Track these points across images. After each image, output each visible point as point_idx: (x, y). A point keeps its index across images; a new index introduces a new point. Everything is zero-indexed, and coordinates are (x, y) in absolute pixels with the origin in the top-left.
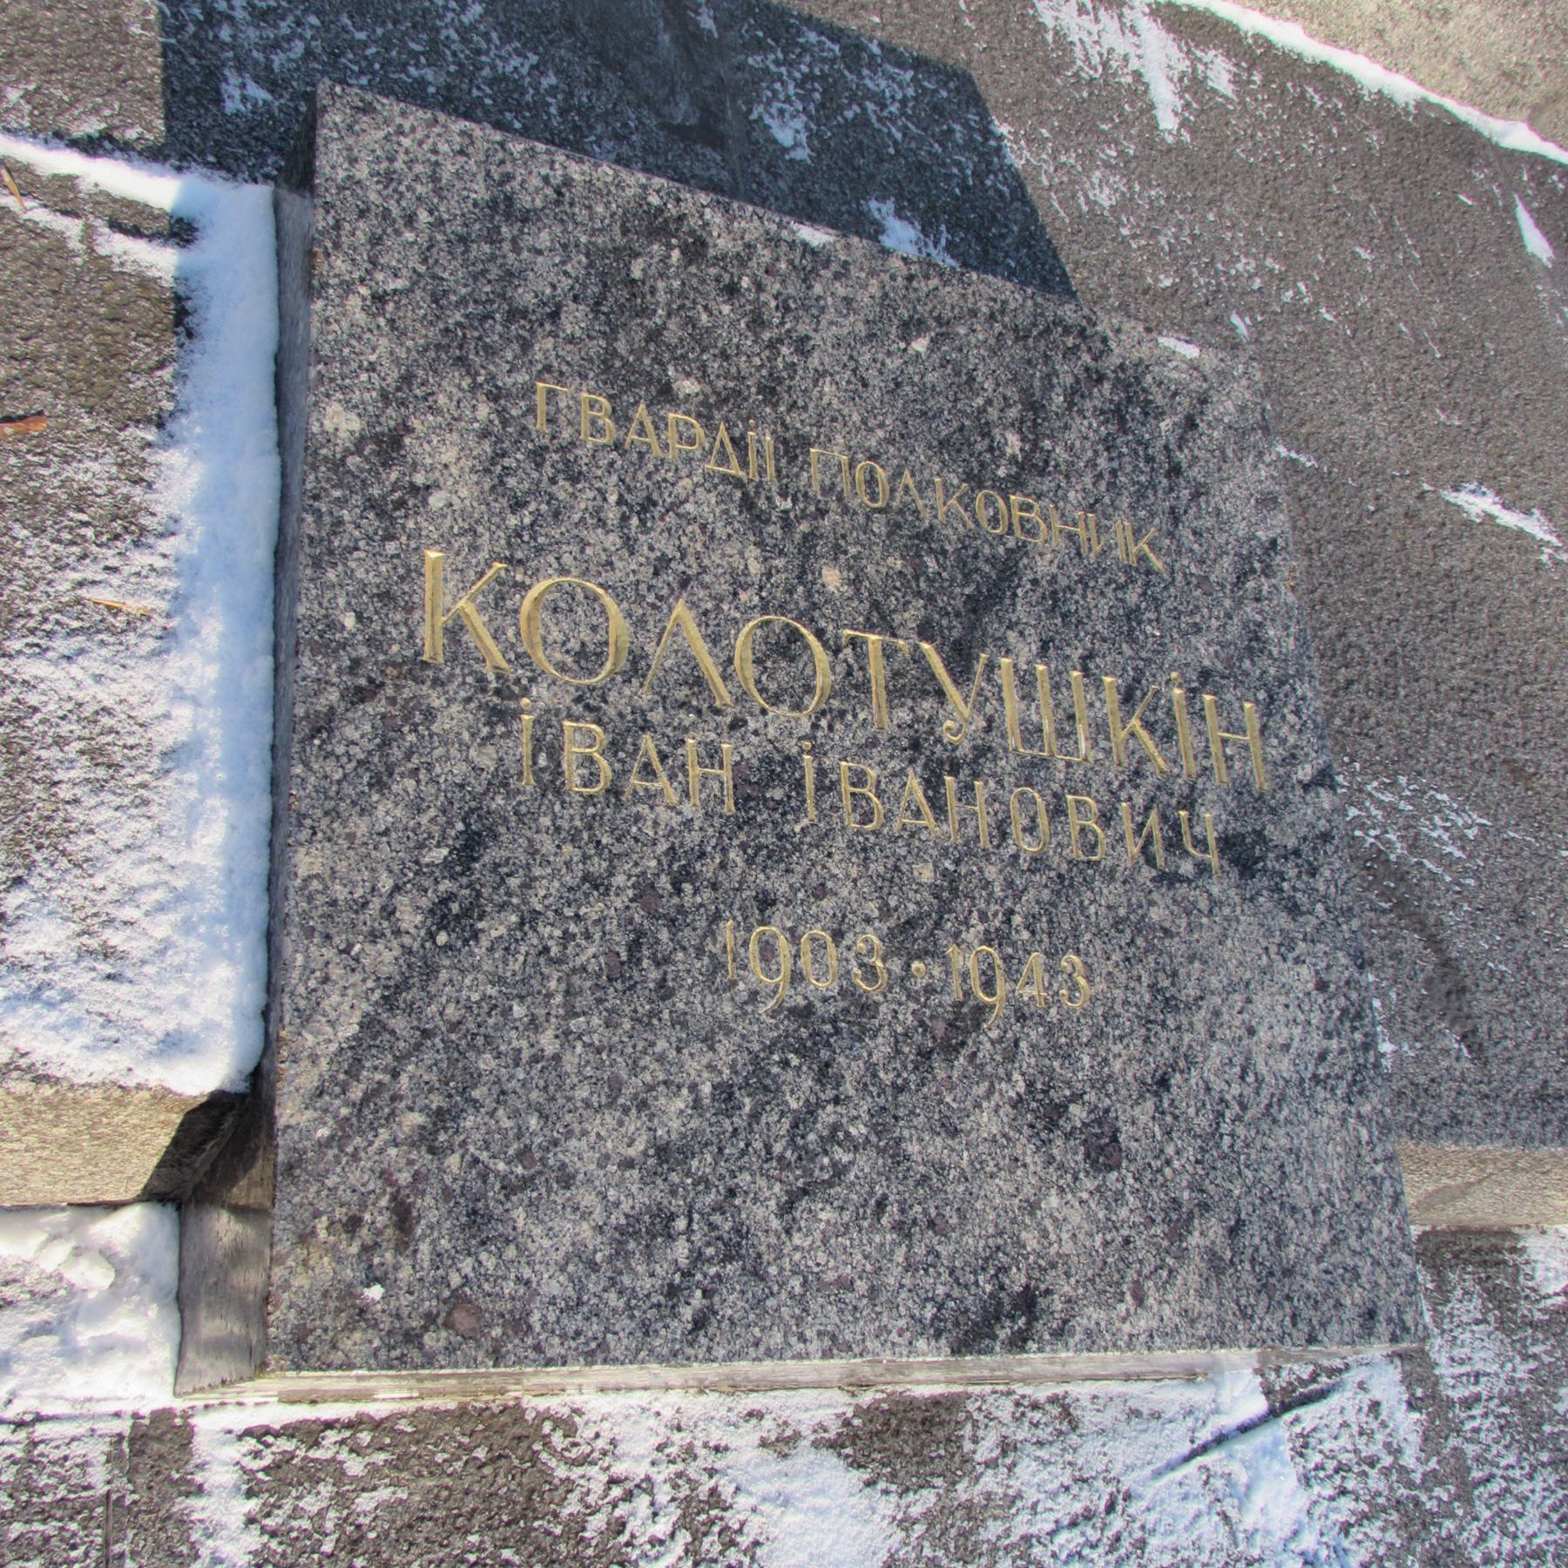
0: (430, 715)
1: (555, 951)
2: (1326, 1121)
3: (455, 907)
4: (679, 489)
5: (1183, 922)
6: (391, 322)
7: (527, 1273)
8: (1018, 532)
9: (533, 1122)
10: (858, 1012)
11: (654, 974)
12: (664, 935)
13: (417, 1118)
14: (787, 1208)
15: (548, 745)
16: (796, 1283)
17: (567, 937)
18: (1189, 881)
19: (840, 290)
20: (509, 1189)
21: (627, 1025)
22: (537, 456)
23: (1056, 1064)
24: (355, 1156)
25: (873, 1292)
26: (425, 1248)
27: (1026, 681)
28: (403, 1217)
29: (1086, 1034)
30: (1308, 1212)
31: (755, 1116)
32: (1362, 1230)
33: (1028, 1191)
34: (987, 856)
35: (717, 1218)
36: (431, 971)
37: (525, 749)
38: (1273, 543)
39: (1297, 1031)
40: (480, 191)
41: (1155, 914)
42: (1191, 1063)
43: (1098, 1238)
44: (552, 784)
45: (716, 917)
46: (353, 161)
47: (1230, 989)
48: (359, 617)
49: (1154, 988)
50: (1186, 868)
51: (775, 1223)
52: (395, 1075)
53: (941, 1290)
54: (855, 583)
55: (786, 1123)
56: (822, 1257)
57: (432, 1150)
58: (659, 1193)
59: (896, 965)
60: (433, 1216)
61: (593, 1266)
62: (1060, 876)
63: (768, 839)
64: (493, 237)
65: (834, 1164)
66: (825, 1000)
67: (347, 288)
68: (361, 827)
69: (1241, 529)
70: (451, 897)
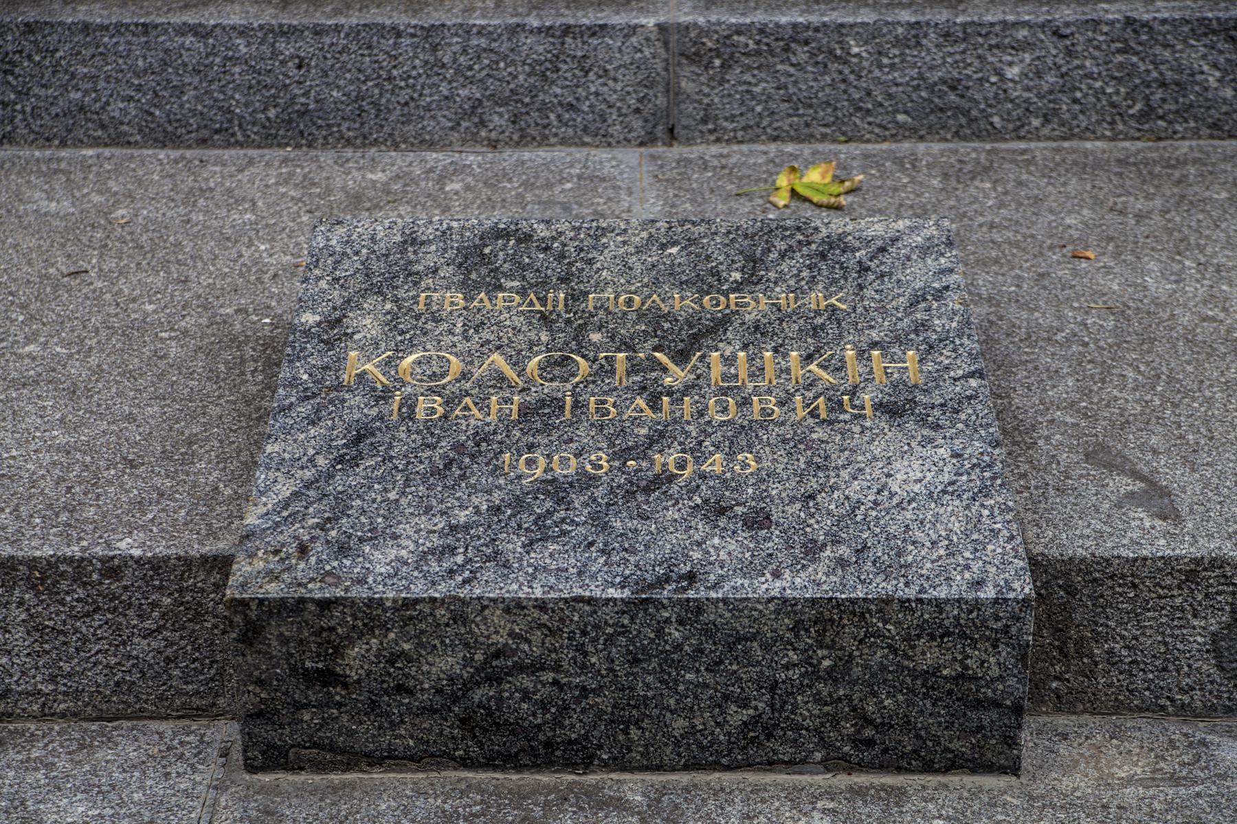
0: (343, 401)
1: (401, 467)
2: (950, 508)
3: (347, 457)
4: (502, 318)
5: (839, 437)
6: (342, 286)
7: (368, 565)
8: (733, 307)
9: (380, 520)
10: (586, 481)
11: (458, 472)
12: (467, 460)
13: (316, 520)
14: (529, 546)
15: (409, 404)
16: (530, 570)
17: (408, 463)
18: (846, 422)
19: (619, 239)
20: (361, 540)
21: (439, 489)
22: (418, 317)
23: (727, 493)
24: (281, 532)
25: (580, 573)
26: (313, 560)
27: (729, 361)
28: (303, 550)
29: (752, 481)
30: (928, 544)
31: (514, 515)
32: (976, 550)
33: (697, 537)
34: (688, 423)
35: (484, 548)
36: (331, 476)
37: (395, 407)
38: (947, 288)
39: (929, 476)
40: (398, 238)
41: (814, 436)
42: (833, 488)
43: (747, 555)
44: (411, 416)
45: (501, 452)
46: (328, 240)
47: (875, 459)
48: (310, 375)
49: (809, 463)
50: (847, 417)
51: (519, 550)
52: (306, 508)
53: (627, 572)
54: (612, 338)
55: (533, 518)
56: (548, 561)
57: (322, 529)
58: (450, 540)
59: (617, 464)
60: (320, 549)
61: (406, 563)
62: (743, 427)
63: (539, 425)
64: (403, 252)
65: (561, 530)
66: (565, 476)
67: (319, 279)
68: (303, 436)
69: (919, 285)
70: (346, 454)
